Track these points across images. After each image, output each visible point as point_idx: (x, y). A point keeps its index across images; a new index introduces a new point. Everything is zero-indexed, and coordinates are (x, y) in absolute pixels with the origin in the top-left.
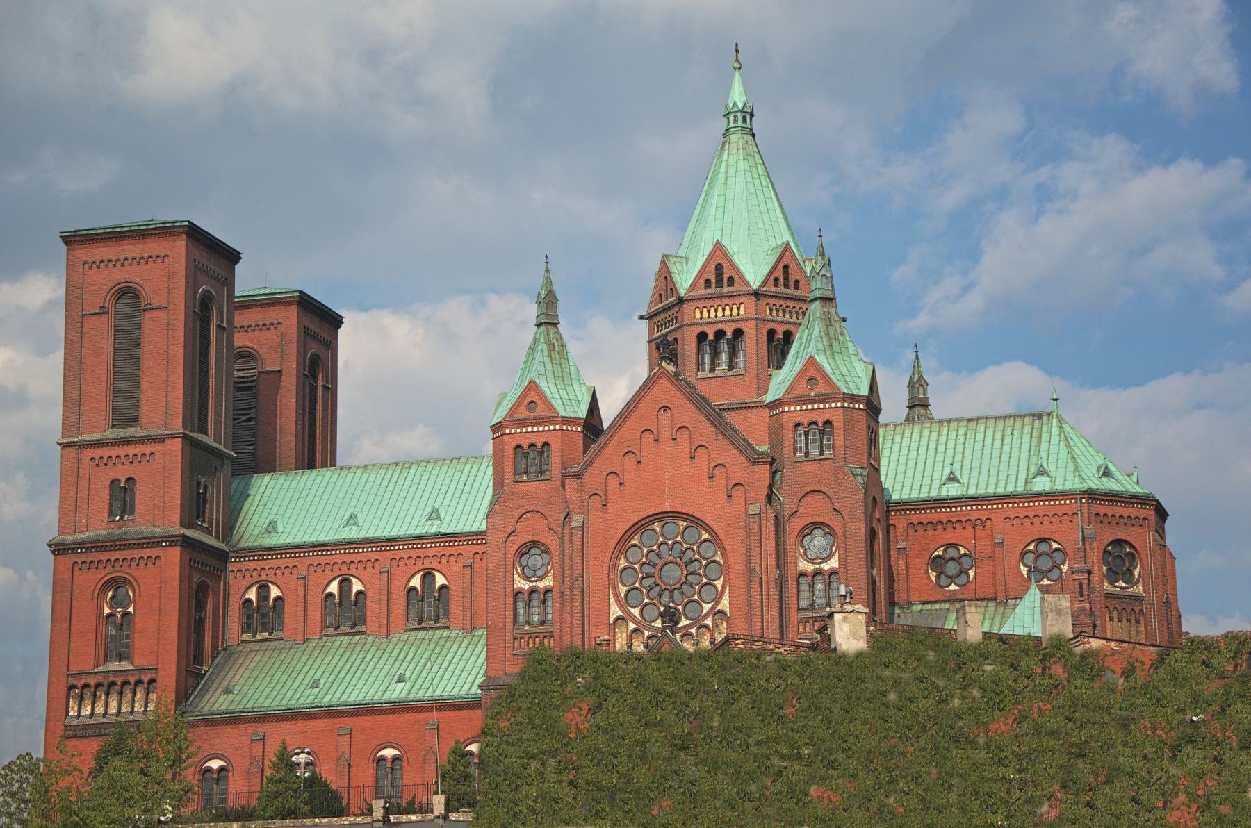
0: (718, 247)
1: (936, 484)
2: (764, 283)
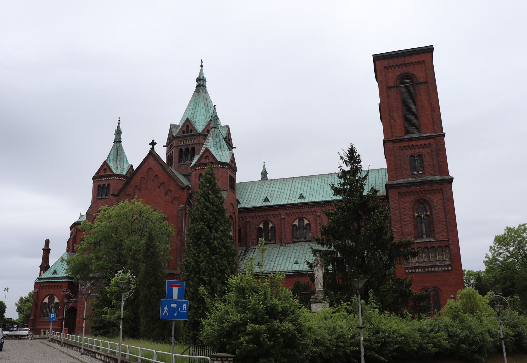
0: (188, 120)
1: (261, 201)
2: (203, 131)
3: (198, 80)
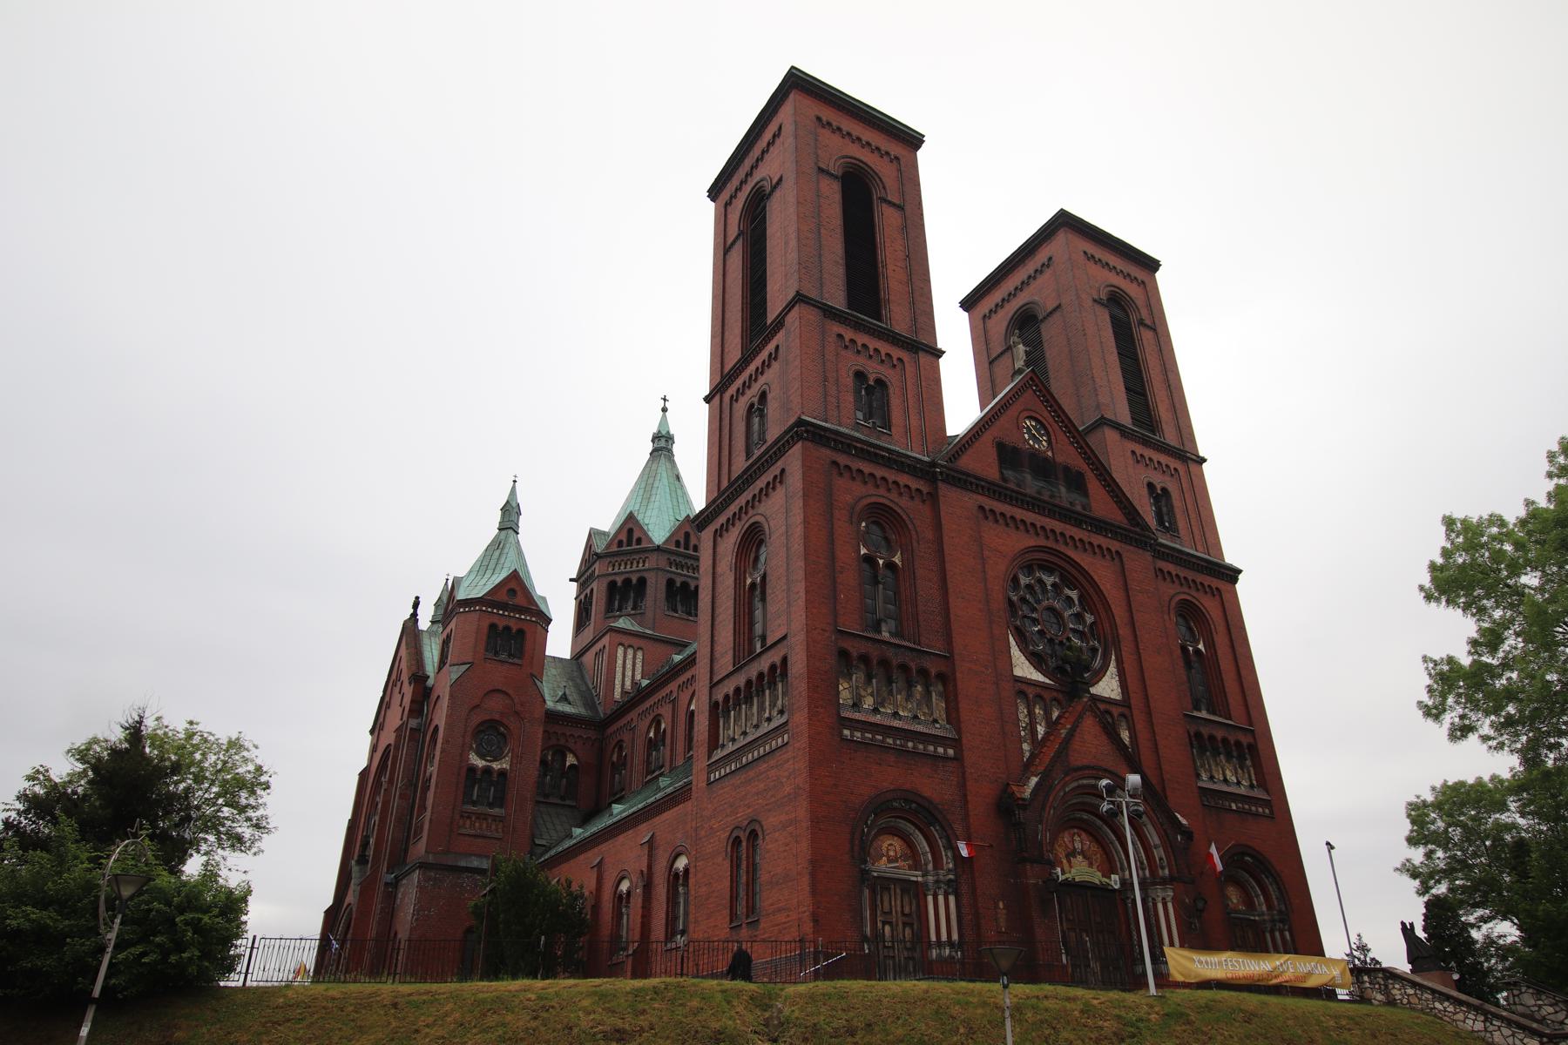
0: (631, 518)
3: (656, 438)
